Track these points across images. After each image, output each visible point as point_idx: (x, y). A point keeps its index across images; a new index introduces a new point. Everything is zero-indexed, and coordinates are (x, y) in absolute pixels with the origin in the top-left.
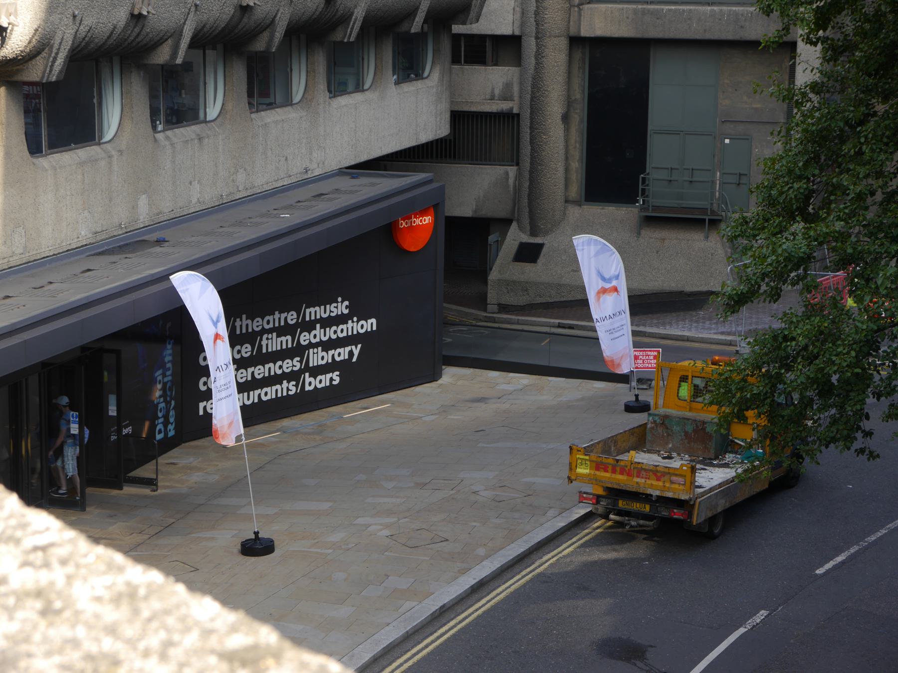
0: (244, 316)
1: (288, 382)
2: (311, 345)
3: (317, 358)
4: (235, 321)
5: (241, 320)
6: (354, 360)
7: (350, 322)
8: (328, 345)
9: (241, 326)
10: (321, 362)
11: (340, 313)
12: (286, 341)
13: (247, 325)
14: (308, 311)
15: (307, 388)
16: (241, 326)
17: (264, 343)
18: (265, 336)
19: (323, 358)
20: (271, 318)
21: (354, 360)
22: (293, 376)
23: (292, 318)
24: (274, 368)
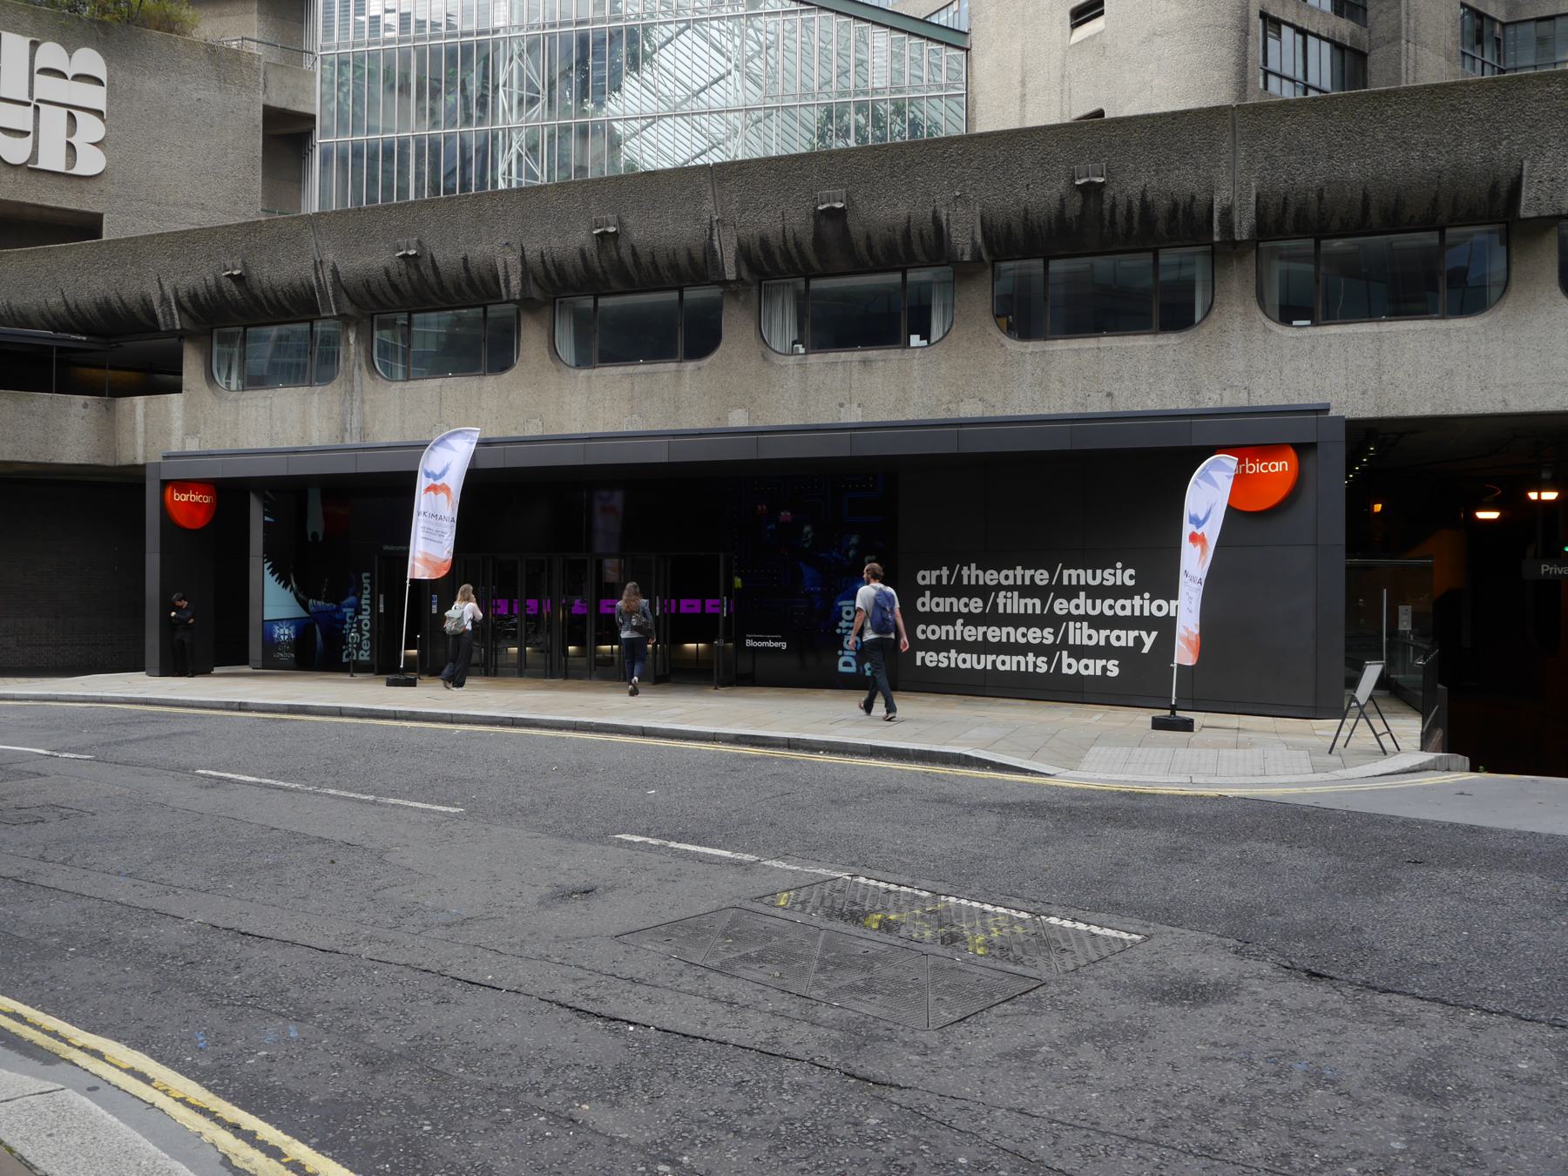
0: (973, 566)
1: (1037, 656)
2: (1069, 617)
3: (1080, 635)
6: (1145, 650)
7: (1137, 598)
8: (1098, 622)
10: (1086, 642)
11: (1119, 583)
14: (1066, 573)
15: (1065, 670)
17: (1001, 601)
18: (1002, 594)
20: (1010, 573)
21: (1145, 650)
22: (1039, 649)
23: (1041, 577)
24: (1017, 635)
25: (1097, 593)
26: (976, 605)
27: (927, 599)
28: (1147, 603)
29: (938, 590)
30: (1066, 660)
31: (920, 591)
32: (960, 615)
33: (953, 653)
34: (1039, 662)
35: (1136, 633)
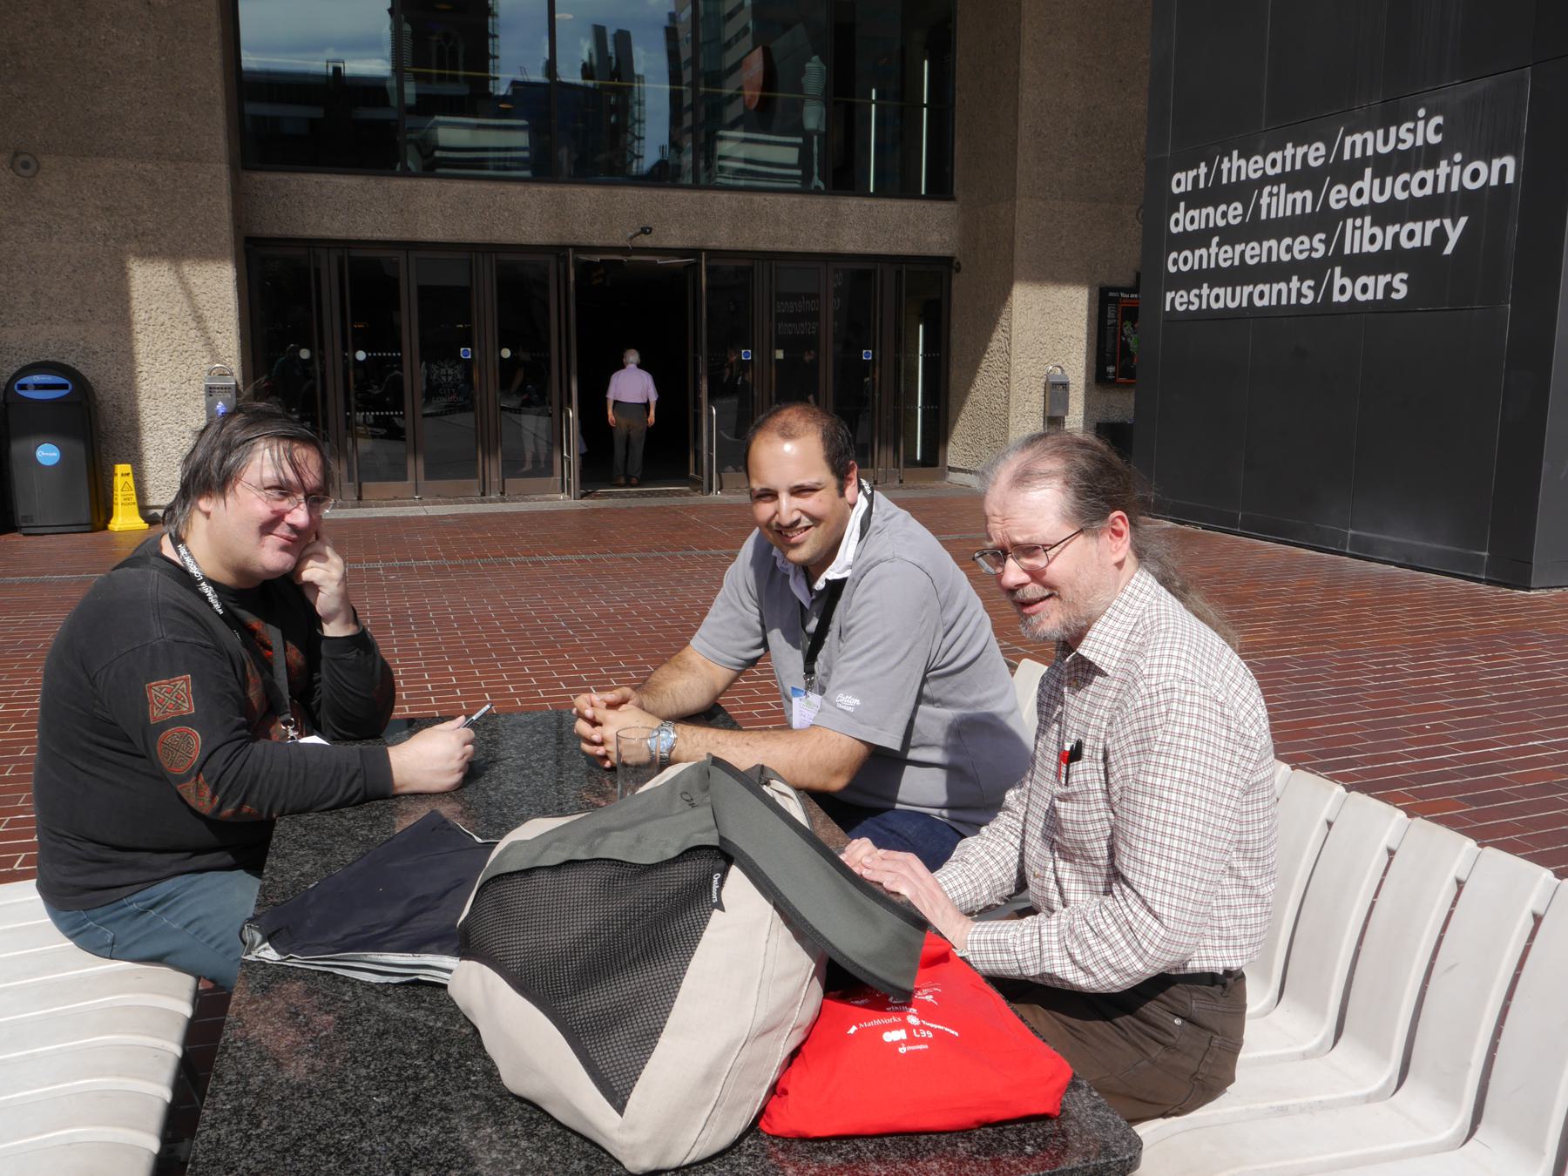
0: (1235, 153)
1: (1301, 280)
2: (1350, 212)
3: (1362, 238)
4: (1221, 162)
5: (1230, 160)
6: (1448, 250)
7: (1443, 163)
8: (1386, 214)
9: (1230, 170)
10: (1367, 248)
11: (1420, 142)
12: (1303, 200)
13: (1239, 168)
14: (1348, 140)
15: (1336, 297)
16: (1230, 170)
17: (1264, 201)
18: (1267, 189)
19: (1373, 239)
20: (1278, 156)
21: (1448, 250)
23: (1315, 154)
25: (1386, 166)
26: (1235, 212)
27: (1179, 215)
28: (1457, 169)
29: (1196, 199)
30: (1338, 281)
31: (1173, 203)
32: (1216, 230)
33: (1205, 290)
34: (1305, 290)
35: (1437, 223)
